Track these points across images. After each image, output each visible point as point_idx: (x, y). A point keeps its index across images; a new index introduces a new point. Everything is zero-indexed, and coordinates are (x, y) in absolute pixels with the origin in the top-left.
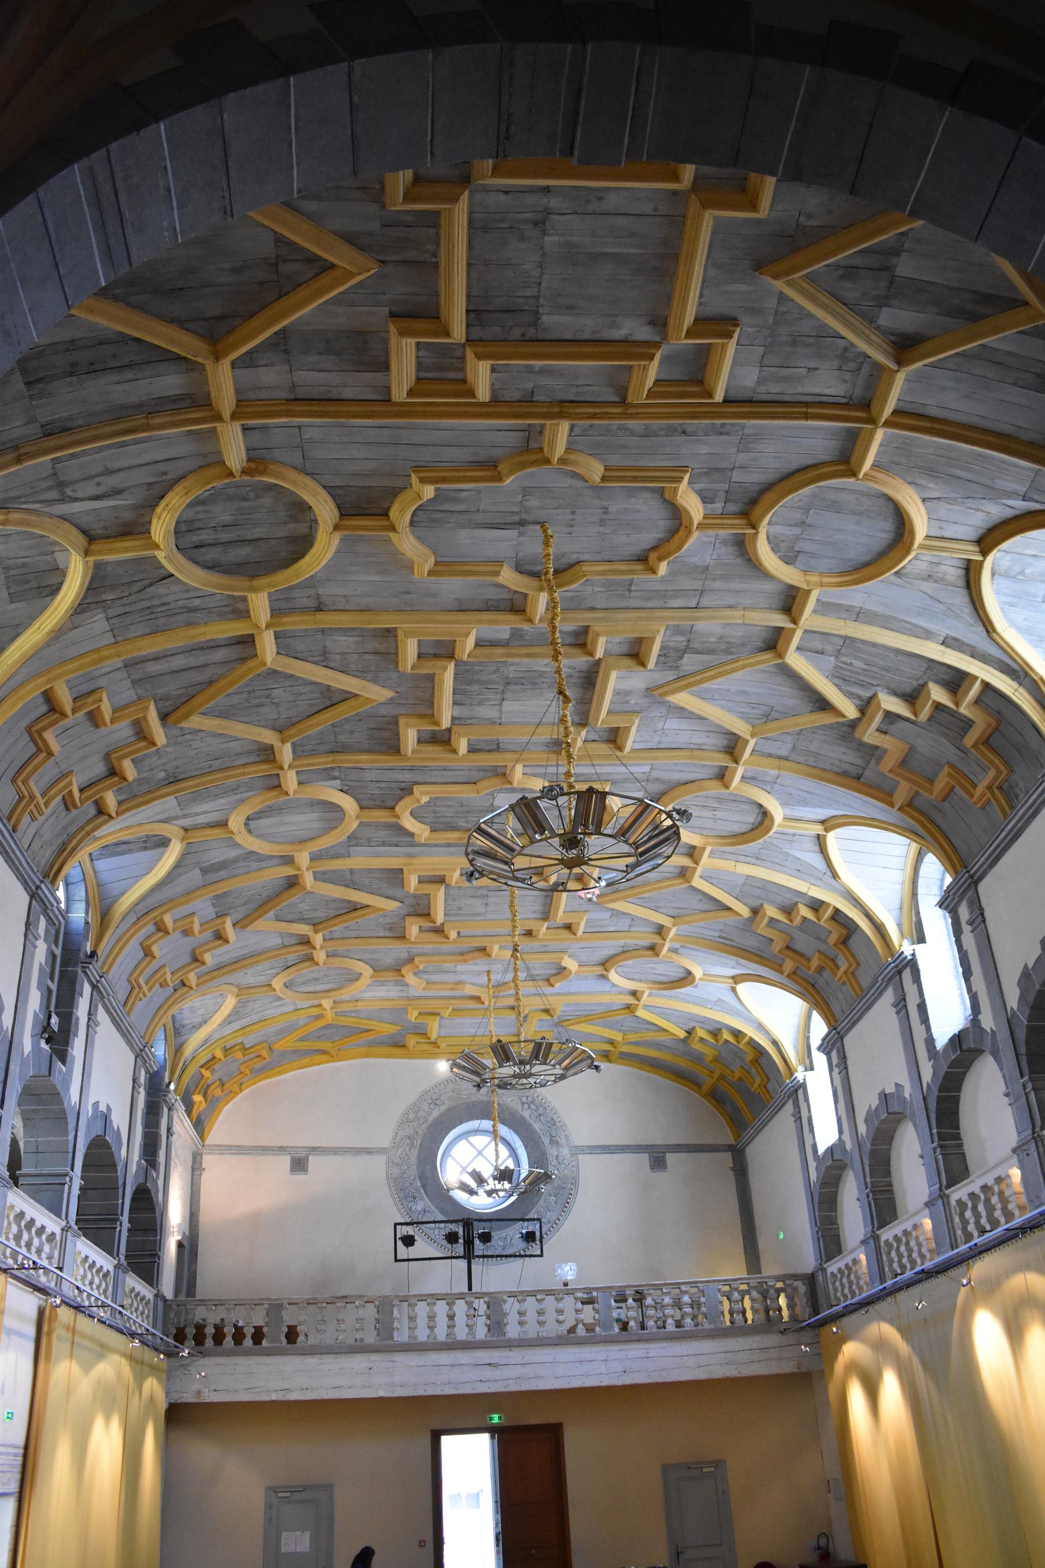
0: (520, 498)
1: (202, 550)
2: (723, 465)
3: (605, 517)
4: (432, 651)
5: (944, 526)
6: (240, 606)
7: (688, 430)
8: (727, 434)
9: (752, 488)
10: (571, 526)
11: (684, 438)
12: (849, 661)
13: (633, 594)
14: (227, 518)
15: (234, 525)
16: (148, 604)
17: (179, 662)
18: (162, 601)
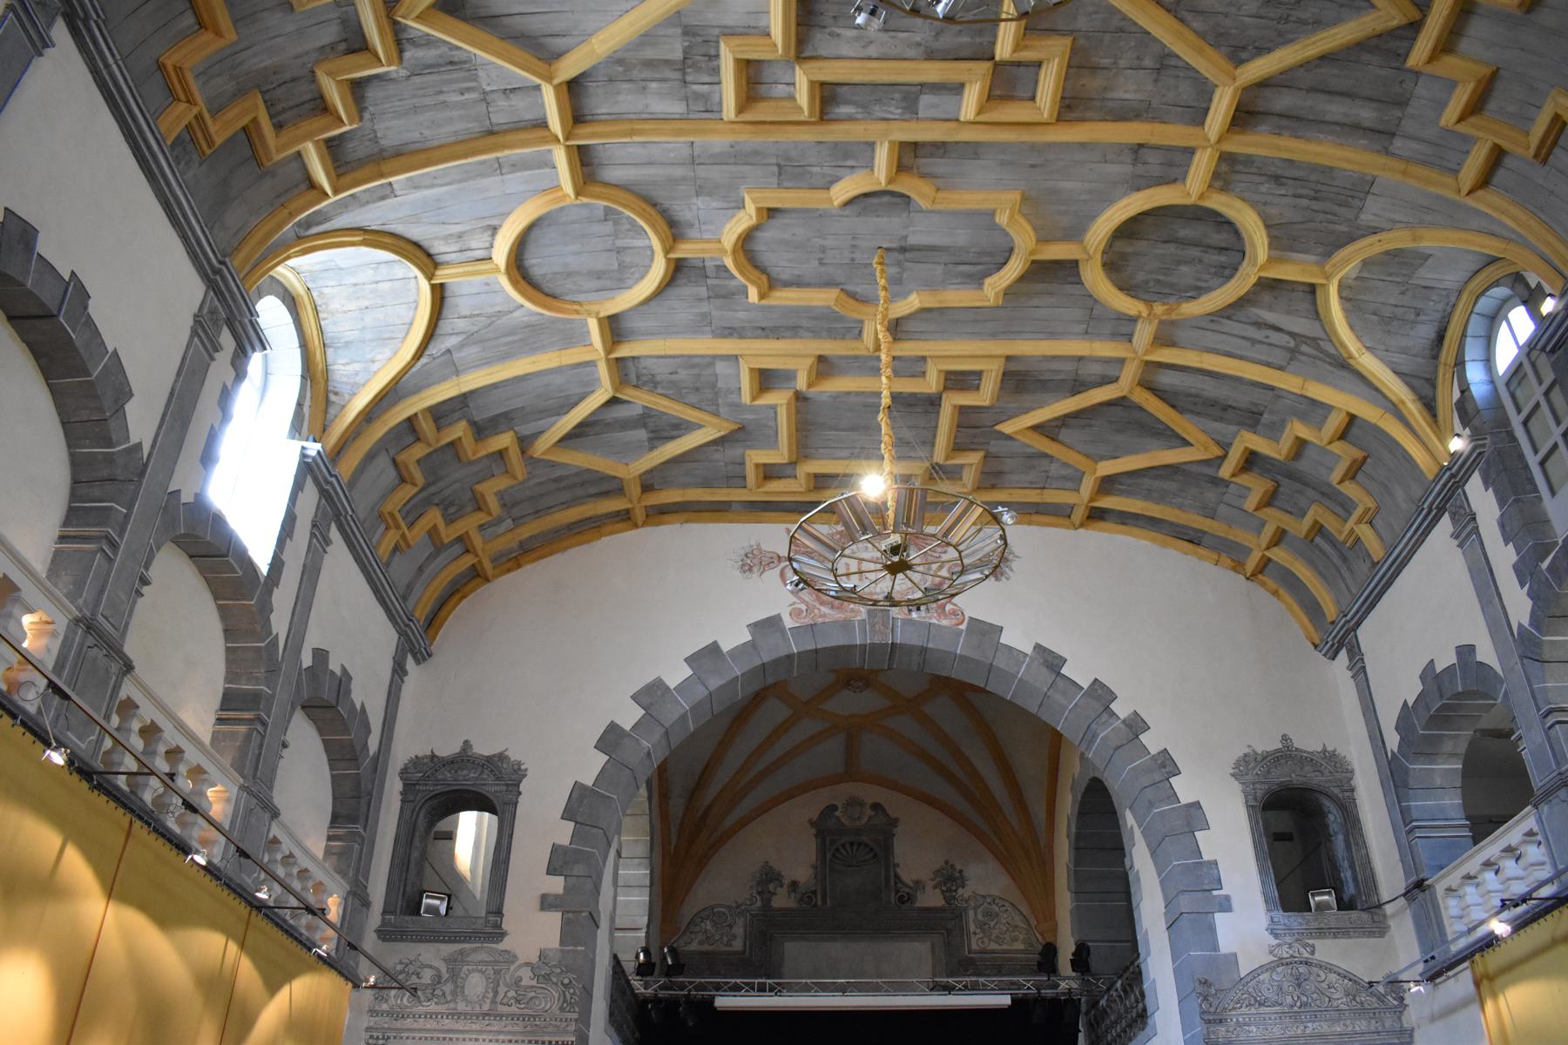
0: (905, 275)
1: (1224, 245)
2: (718, 302)
3: (821, 256)
4: (1022, 69)
5: (487, 287)
6: (1224, 168)
7: (760, 331)
8: (725, 328)
9: (685, 281)
10: (854, 246)
11: (763, 326)
12: (467, 96)
13: (774, 160)
14: (1184, 269)
15: (1179, 263)
16: (1315, 205)
17: (1336, 109)
18: (1298, 201)
